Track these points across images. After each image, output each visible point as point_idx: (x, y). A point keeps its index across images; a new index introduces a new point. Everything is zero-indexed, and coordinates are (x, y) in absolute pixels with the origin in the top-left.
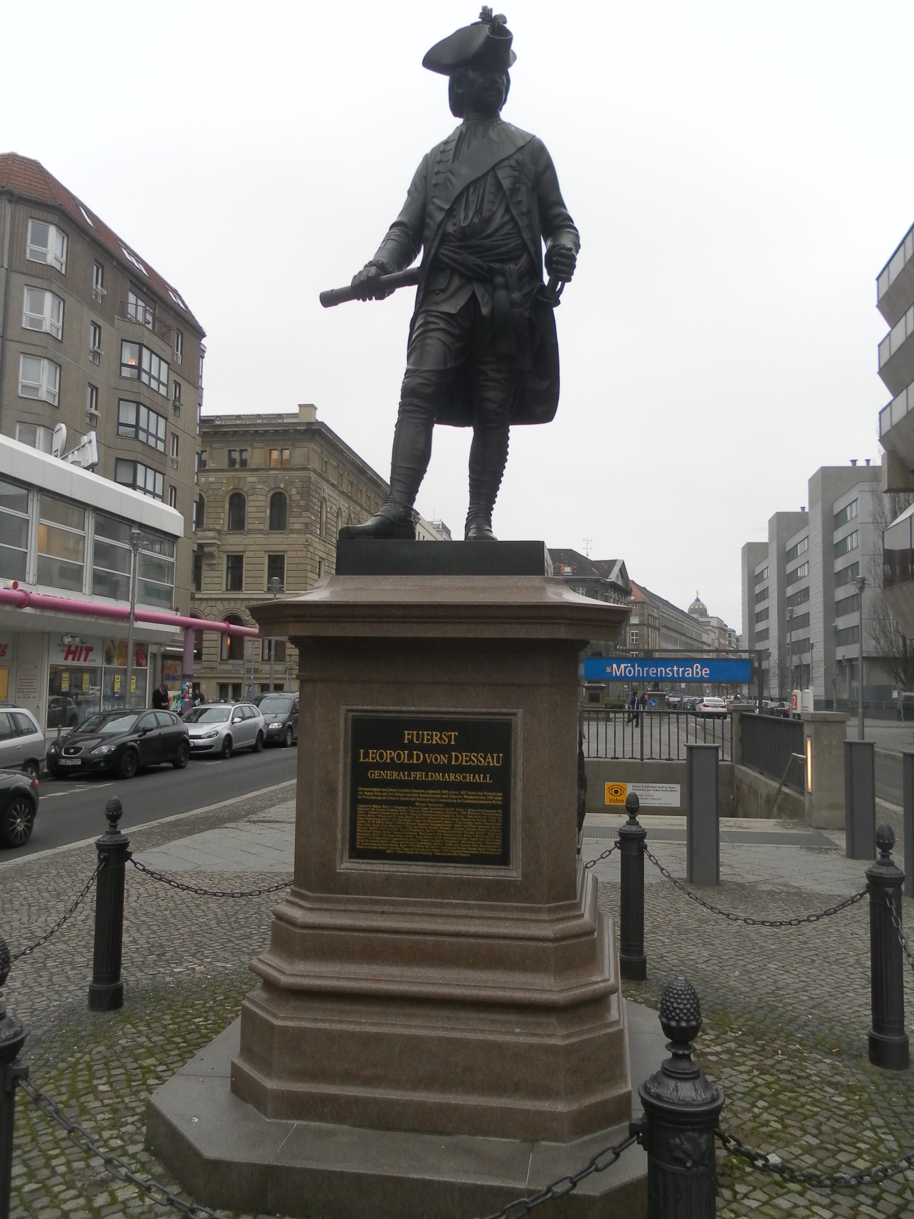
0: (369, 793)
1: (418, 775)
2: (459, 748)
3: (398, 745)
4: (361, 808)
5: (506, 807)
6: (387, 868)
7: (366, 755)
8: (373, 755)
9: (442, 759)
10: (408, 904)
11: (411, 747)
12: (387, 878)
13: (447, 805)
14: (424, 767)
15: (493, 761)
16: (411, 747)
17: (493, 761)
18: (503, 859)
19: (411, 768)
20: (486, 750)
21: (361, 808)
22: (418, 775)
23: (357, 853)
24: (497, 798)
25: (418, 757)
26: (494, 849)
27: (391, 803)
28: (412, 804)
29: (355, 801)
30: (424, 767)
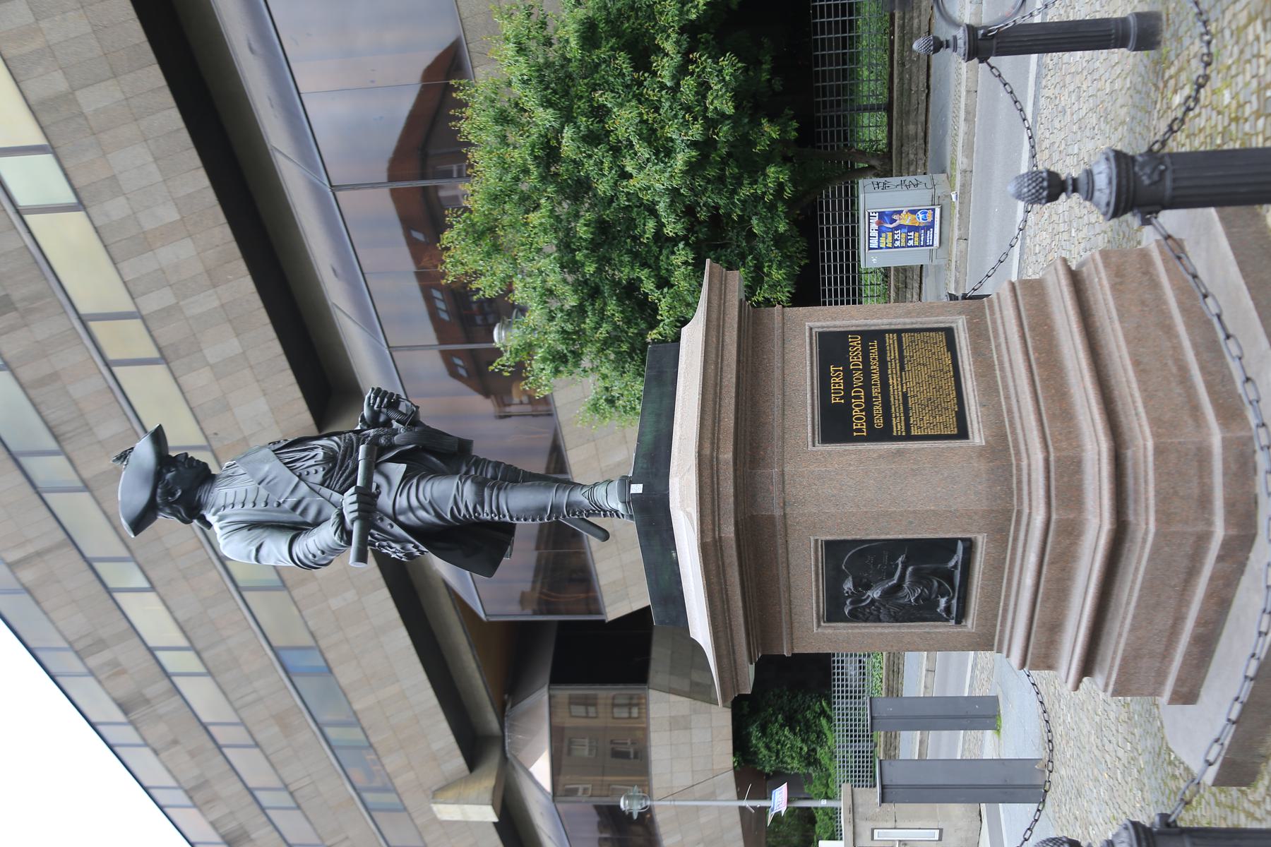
0: (898, 427)
1: (876, 391)
2: (846, 363)
3: (847, 408)
4: (914, 432)
5: (899, 332)
6: (973, 408)
7: (860, 430)
8: (859, 425)
9: (857, 374)
10: (1006, 387)
11: (847, 397)
12: (983, 406)
13: (902, 369)
14: (867, 386)
15: (856, 343)
16: (847, 397)
17: (856, 343)
18: (949, 333)
19: (869, 398)
20: (846, 346)
21: (914, 432)
22: (876, 391)
23: (963, 433)
24: (890, 340)
25: (858, 391)
26: (941, 337)
27: (906, 410)
28: (905, 396)
29: (909, 437)
30: (867, 386)
